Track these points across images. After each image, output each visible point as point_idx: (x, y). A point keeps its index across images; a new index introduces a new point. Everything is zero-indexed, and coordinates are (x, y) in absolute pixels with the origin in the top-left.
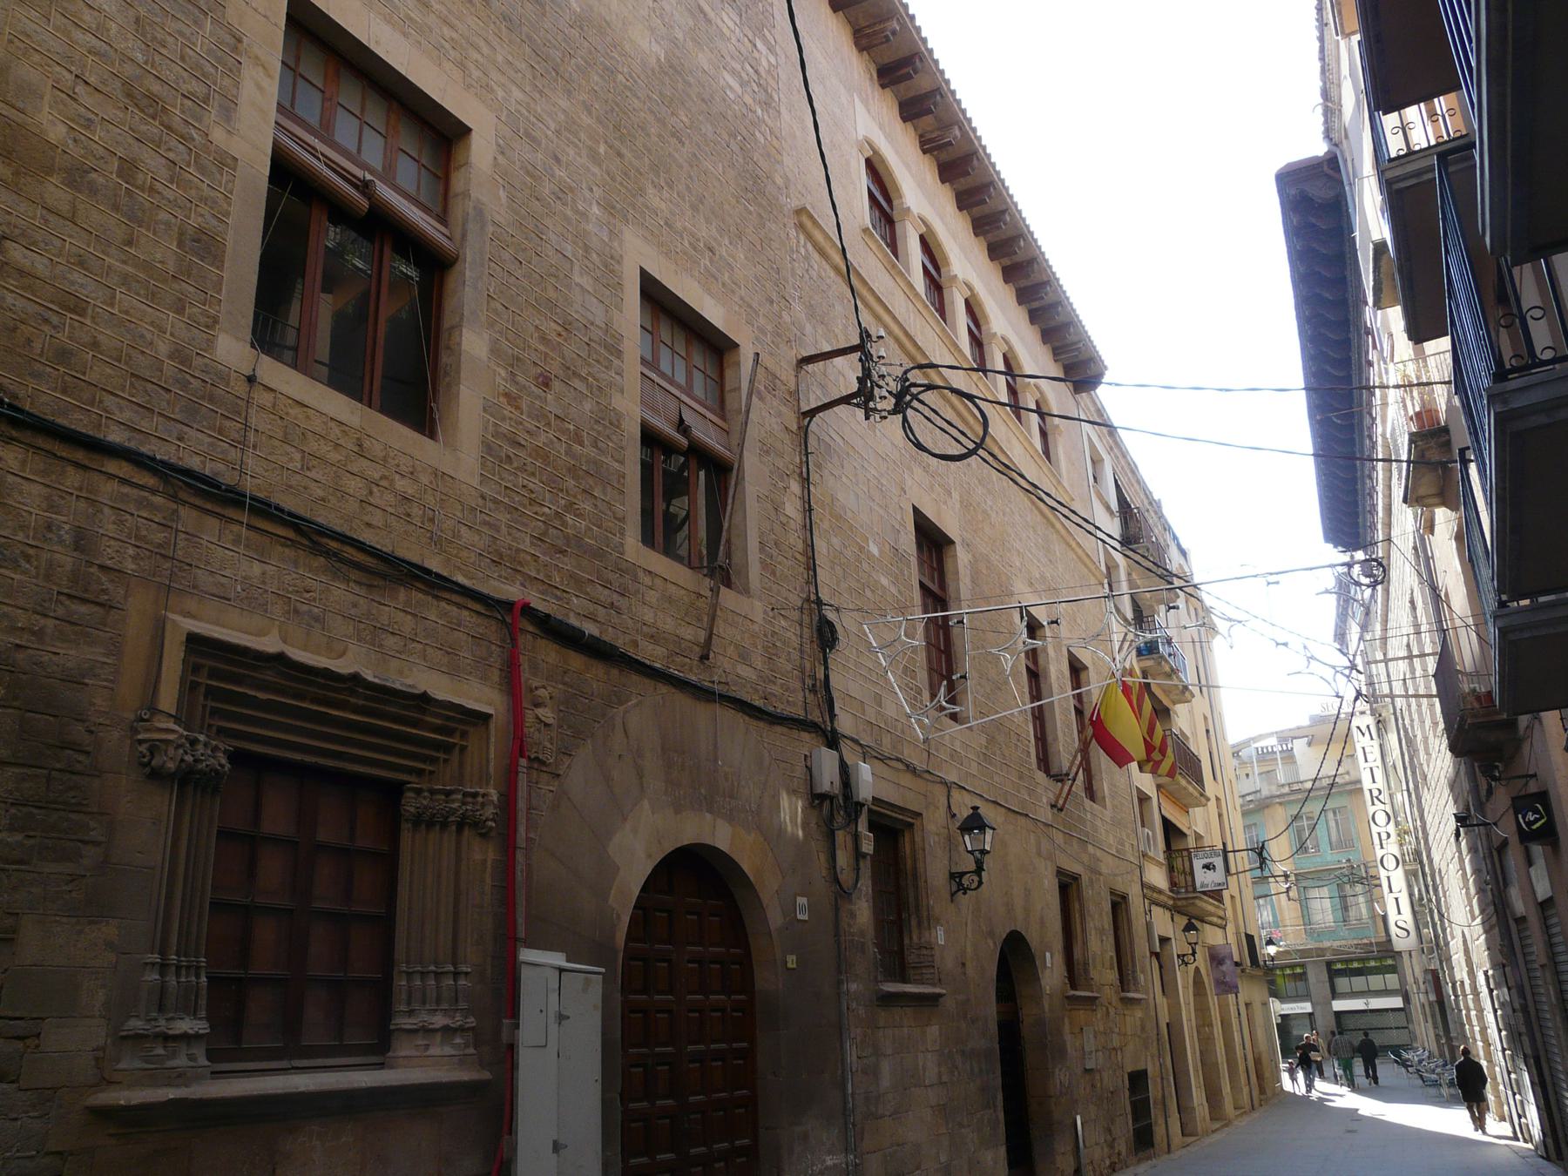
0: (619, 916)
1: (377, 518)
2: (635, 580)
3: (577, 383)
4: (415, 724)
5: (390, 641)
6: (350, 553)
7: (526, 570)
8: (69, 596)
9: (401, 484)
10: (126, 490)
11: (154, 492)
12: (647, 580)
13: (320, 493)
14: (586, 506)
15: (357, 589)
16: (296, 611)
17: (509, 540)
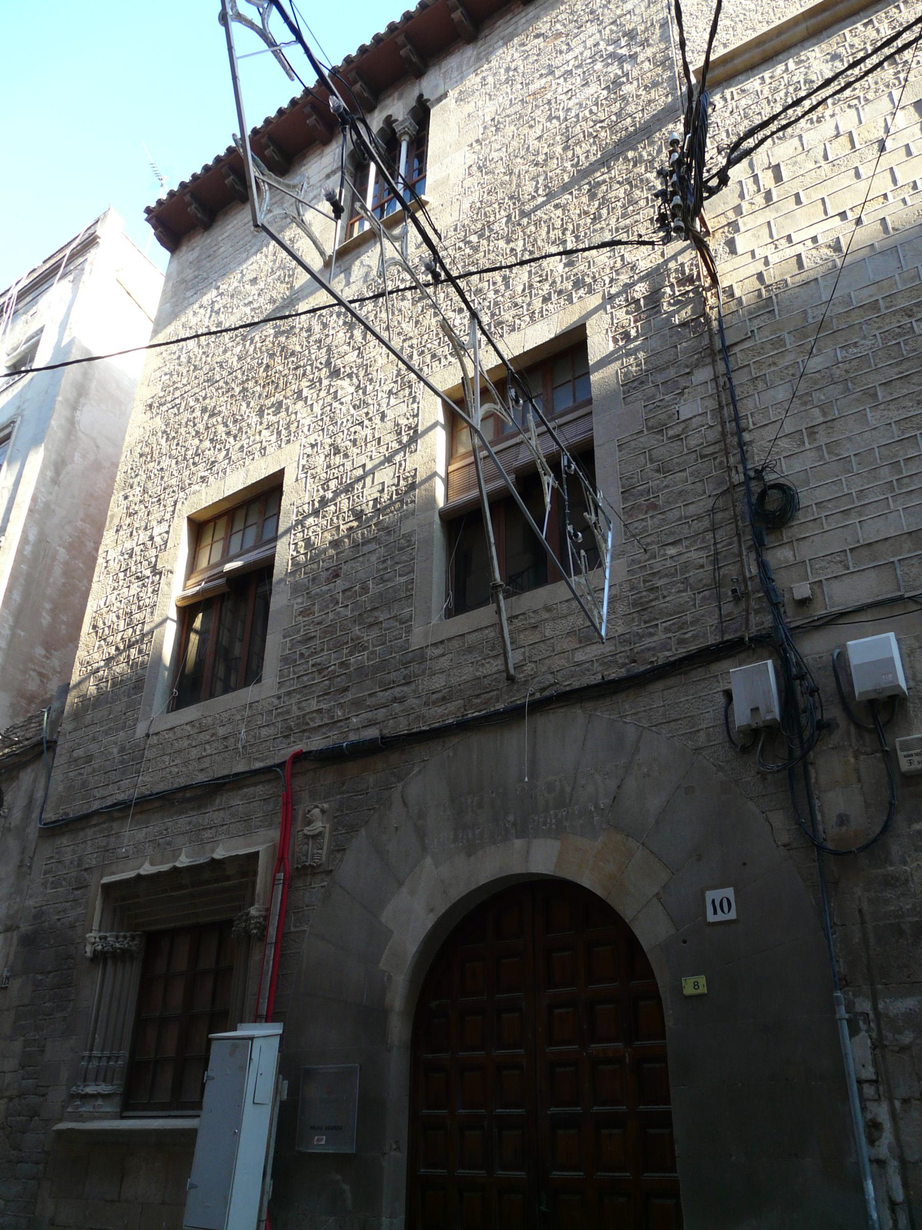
0: (390, 978)
1: (206, 763)
3: (366, 549)
4: (228, 878)
5: (207, 834)
6: (188, 795)
7: (312, 725)
9: (221, 732)
10: (97, 828)
11: (104, 823)
12: (438, 651)
13: (176, 770)
14: (375, 633)
15: (192, 813)
16: (159, 845)
17: (299, 713)
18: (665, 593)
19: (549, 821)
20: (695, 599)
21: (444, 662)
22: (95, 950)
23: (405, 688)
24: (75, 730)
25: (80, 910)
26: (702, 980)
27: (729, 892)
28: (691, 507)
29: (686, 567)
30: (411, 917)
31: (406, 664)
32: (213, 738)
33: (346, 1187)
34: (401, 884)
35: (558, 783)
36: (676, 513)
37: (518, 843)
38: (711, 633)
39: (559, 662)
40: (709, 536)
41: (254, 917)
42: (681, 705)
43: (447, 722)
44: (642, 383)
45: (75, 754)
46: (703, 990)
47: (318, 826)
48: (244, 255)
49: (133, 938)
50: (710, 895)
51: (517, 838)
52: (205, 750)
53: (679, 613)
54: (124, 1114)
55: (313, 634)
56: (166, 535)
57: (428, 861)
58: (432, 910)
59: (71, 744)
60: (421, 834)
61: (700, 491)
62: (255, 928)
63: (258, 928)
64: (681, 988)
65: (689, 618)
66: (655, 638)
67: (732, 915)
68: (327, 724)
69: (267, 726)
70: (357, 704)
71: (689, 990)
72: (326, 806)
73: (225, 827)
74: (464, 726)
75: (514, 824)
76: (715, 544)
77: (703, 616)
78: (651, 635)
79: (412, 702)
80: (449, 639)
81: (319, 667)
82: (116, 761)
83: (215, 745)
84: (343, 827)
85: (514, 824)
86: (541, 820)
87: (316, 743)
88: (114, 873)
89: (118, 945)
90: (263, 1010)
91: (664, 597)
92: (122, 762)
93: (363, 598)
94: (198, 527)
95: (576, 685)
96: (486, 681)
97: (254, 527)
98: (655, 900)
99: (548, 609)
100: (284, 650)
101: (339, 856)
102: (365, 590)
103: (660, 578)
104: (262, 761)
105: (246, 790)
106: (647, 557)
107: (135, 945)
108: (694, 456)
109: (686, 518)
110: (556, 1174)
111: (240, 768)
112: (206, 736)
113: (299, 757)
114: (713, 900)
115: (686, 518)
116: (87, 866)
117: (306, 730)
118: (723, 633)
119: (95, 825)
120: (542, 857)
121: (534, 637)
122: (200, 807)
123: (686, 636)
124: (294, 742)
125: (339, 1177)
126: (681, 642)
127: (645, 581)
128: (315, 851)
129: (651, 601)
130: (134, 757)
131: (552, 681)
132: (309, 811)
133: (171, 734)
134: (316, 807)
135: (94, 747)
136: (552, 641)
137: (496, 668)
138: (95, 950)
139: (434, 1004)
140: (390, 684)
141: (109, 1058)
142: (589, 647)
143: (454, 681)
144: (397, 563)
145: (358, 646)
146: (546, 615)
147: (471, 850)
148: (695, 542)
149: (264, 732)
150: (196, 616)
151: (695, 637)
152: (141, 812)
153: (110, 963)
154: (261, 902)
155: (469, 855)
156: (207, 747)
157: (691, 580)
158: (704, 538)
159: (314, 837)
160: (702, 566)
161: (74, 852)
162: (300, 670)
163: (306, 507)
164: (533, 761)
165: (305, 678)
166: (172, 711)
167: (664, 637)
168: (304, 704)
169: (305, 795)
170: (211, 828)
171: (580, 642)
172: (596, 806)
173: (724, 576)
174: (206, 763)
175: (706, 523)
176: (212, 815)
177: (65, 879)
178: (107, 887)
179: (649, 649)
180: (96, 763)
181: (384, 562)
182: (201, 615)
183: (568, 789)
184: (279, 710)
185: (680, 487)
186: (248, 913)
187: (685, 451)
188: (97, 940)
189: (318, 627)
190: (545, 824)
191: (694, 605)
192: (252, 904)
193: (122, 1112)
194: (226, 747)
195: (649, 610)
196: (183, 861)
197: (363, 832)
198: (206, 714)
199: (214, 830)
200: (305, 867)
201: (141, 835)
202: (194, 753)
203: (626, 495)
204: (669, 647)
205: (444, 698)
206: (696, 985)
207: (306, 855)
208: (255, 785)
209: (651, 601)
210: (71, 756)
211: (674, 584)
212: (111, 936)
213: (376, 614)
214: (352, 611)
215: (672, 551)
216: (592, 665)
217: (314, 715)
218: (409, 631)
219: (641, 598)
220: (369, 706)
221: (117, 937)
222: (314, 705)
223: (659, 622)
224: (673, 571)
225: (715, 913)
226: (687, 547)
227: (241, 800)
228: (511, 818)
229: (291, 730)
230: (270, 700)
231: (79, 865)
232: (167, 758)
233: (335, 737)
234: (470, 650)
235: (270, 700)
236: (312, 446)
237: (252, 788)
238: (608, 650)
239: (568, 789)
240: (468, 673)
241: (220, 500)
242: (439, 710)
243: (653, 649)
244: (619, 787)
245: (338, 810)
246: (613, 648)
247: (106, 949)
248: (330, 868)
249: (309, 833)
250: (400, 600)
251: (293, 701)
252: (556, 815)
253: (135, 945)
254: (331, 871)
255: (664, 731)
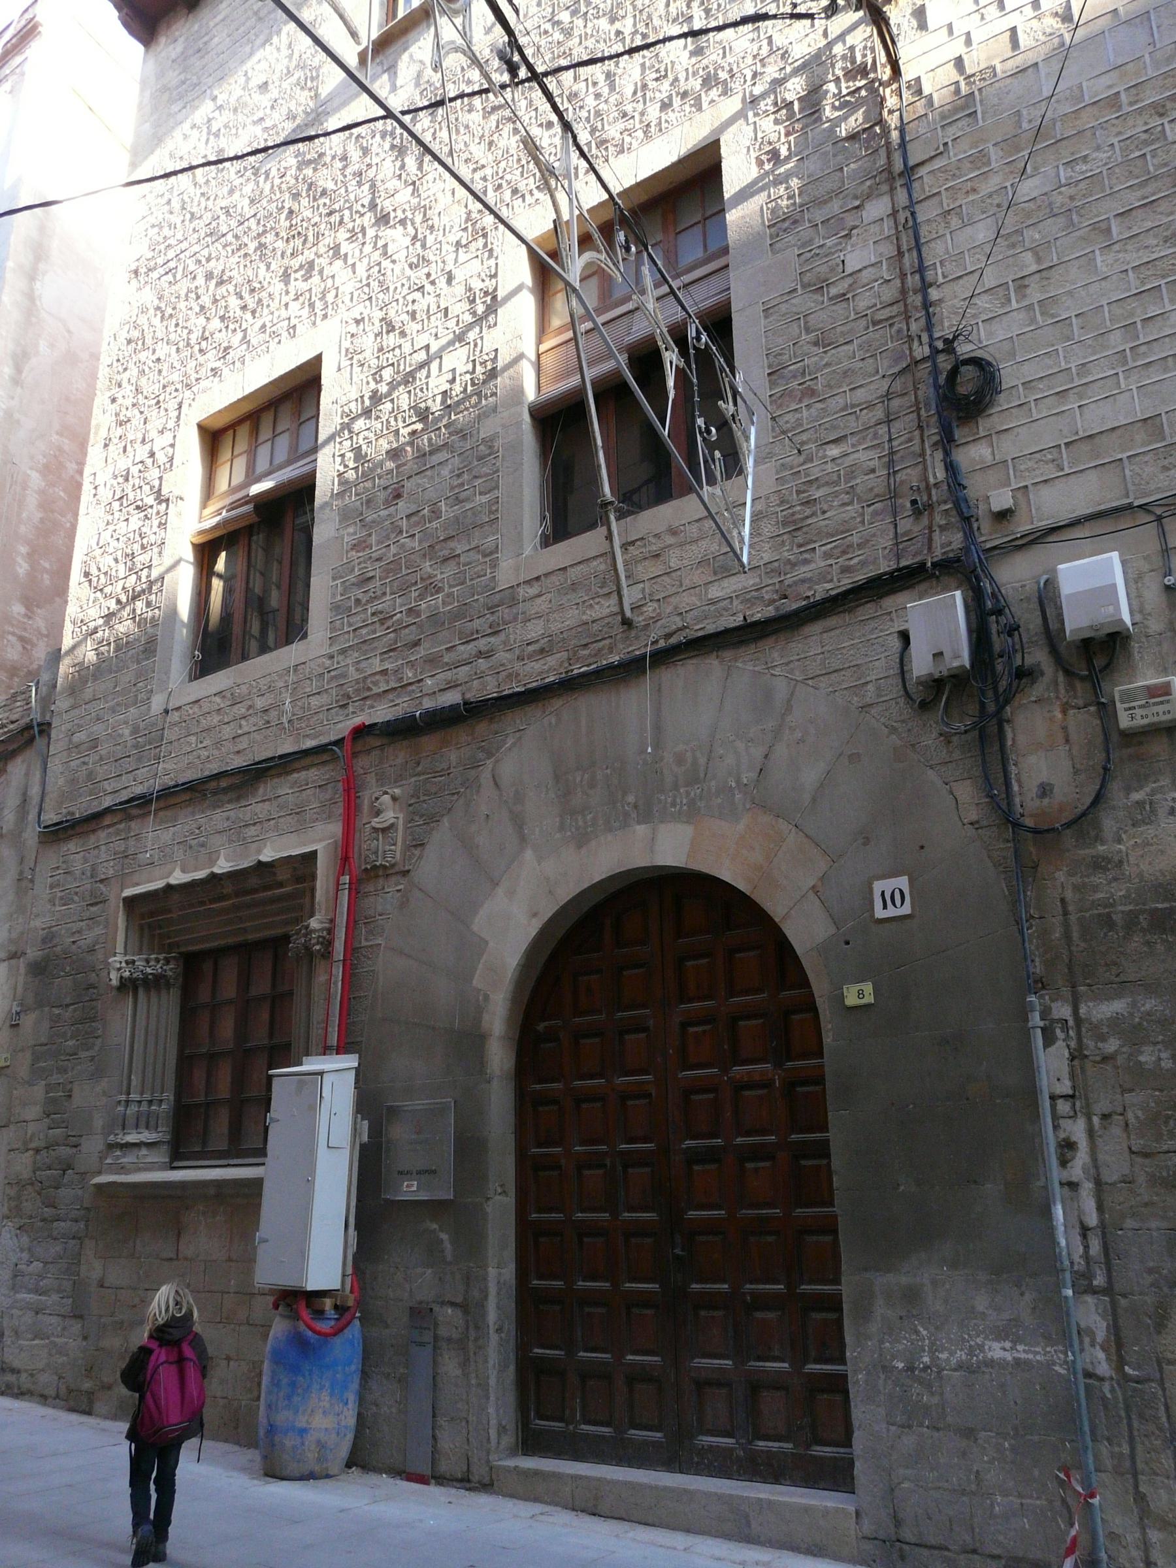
1: (243, 743)
2: (513, 601)
4: (281, 885)
5: (252, 831)
6: (224, 783)
7: (376, 690)
8: (91, 905)
9: (260, 703)
10: (110, 830)
11: (120, 822)
12: (532, 591)
14: (450, 570)
15: (230, 806)
16: (191, 847)
17: (357, 676)
18: (825, 507)
19: (678, 801)
20: (863, 515)
21: (541, 605)
22: (121, 977)
23: (492, 639)
24: (73, 707)
25: (99, 931)
26: (868, 988)
27: (903, 882)
28: (859, 392)
29: (851, 473)
30: (510, 924)
31: (492, 609)
32: (251, 711)
33: (444, 1236)
34: (496, 884)
35: (689, 754)
36: (840, 401)
37: (641, 830)
38: (884, 557)
39: (687, 600)
40: (883, 430)
41: (315, 931)
42: (844, 651)
43: (547, 680)
44: (795, 222)
45: (77, 738)
46: (869, 999)
47: (389, 816)
48: (248, 49)
49: (167, 961)
50: (878, 886)
51: (639, 823)
52: (240, 727)
53: (843, 532)
54: (175, 1164)
55: (371, 574)
56: (170, 450)
57: (529, 855)
58: (535, 915)
59: (68, 726)
60: (518, 822)
61: (871, 369)
62: (318, 943)
63: (322, 944)
64: (842, 997)
65: (855, 539)
66: (813, 566)
67: (906, 909)
68: (394, 689)
69: (318, 693)
70: (432, 661)
71: (851, 1000)
72: (397, 791)
73: (272, 822)
74: (569, 685)
75: (636, 807)
76: (890, 440)
77: (874, 535)
78: (806, 562)
79: (502, 656)
80: (546, 575)
81: (381, 616)
82: (129, 744)
83: (253, 720)
84: (422, 816)
85: (636, 807)
86: (669, 800)
87: (381, 713)
88: (138, 884)
89: (149, 970)
90: (333, 1040)
91: (824, 512)
92: (136, 746)
93: (434, 524)
94: (214, 438)
95: (711, 628)
96: (596, 627)
97: (287, 435)
98: (811, 895)
99: (673, 532)
100: (334, 595)
101: (417, 852)
102: (436, 513)
103: (818, 488)
104: (315, 737)
105: (295, 775)
106: (801, 459)
107: (171, 969)
108: (863, 322)
109: (853, 406)
110: (692, 1214)
111: (287, 747)
112: (241, 710)
113: (360, 732)
114: (883, 892)
115: (853, 406)
116: (103, 877)
117: (368, 697)
118: (898, 557)
119: (109, 826)
120: (670, 847)
121: (655, 569)
122: (238, 799)
123: (852, 562)
124: (353, 713)
125: (435, 1226)
126: (846, 570)
127: (798, 492)
128: (388, 848)
129: (807, 517)
130: (151, 740)
131: (680, 625)
132: (377, 799)
133: (196, 708)
134: (386, 793)
135: (98, 729)
136: (679, 573)
137: (608, 610)
138: (121, 977)
139: (541, 1027)
140: (472, 634)
141: (150, 1102)
142: (726, 580)
143: (555, 627)
144: (476, 477)
145: (430, 587)
146: (670, 540)
147: (582, 840)
148: (864, 439)
149: (315, 702)
150: (217, 556)
151: (863, 564)
152: (166, 808)
153: (141, 992)
154: (323, 912)
155: (579, 847)
156: (243, 722)
157: (859, 490)
158: (876, 434)
159: (384, 830)
160: (873, 471)
161: (86, 861)
162: (357, 621)
163: (353, 406)
164: (658, 728)
165: (364, 631)
166: (196, 679)
167: (823, 564)
168: (363, 665)
169: (371, 779)
170: (255, 824)
171: (715, 573)
172: (738, 782)
173: (902, 482)
174: (243, 743)
175: (879, 413)
176: (256, 807)
177: (76, 893)
178: (131, 903)
179: (803, 581)
180: (103, 749)
181: (458, 476)
182: (223, 554)
183: (702, 761)
184: (332, 673)
185: (845, 364)
186: (307, 927)
187: (853, 316)
188: (124, 965)
189: (378, 565)
190: (674, 804)
191: (863, 522)
192: (312, 915)
193: (171, 1162)
194: (268, 722)
195: (804, 530)
196: (223, 866)
197: (445, 820)
198: (239, 681)
199: (258, 827)
200: (375, 867)
201: (166, 836)
202: (228, 732)
203: (774, 377)
204: (829, 577)
205: (542, 651)
206: (861, 994)
207: (376, 853)
208: (306, 768)
209: (807, 517)
210: (70, 740)
211: (836, 494)
212: (140, 959)
213: (451, 544)
214: (420, 542)
215: (834, 451)
216: (731, 603)
217: (377, 677)
218: (494, 565)
219: (793, 514)
220: (447, 664)
221: (147, 961)
222: (377, 665)
223: (816, 545)
224: (835, 478)
225: (885, 907)
226: (853, 446)
227: (291, 788)
228: (631, 799)
229: (349, 697)
230: (320, 661)
231: (92, 877)
232: (193, 739)
233: (405, 705)
234: (574, 587)
235: (320, 661)
236: (357, 322)
237: (304, 773)
238: (751, 582)
239: (702, 761)
240: (572, 617)
241: (239, 400)
242: (537, 666)
243: (810, 580)
244: (766, 756)
245: (412, 796)
246: (758, 580)
247: (135, 975)
248: (407, 868)
249: (378, 826)
250: (481, 525)
251: (349, 661)
252: (688, 793)
253: (170, 970)
254: (408, 871)
255: (822, 685)
